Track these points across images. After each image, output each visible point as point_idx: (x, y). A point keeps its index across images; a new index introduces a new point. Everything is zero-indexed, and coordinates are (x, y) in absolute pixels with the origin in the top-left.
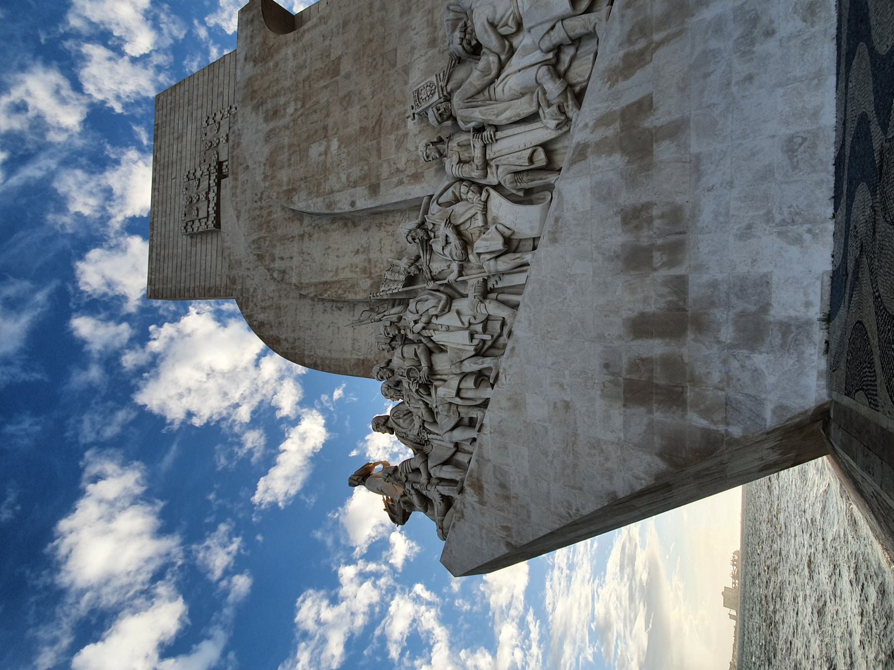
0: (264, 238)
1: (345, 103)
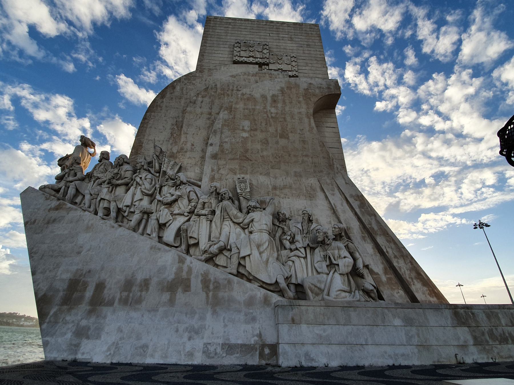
0: (216, 92)
1: (264, 141)
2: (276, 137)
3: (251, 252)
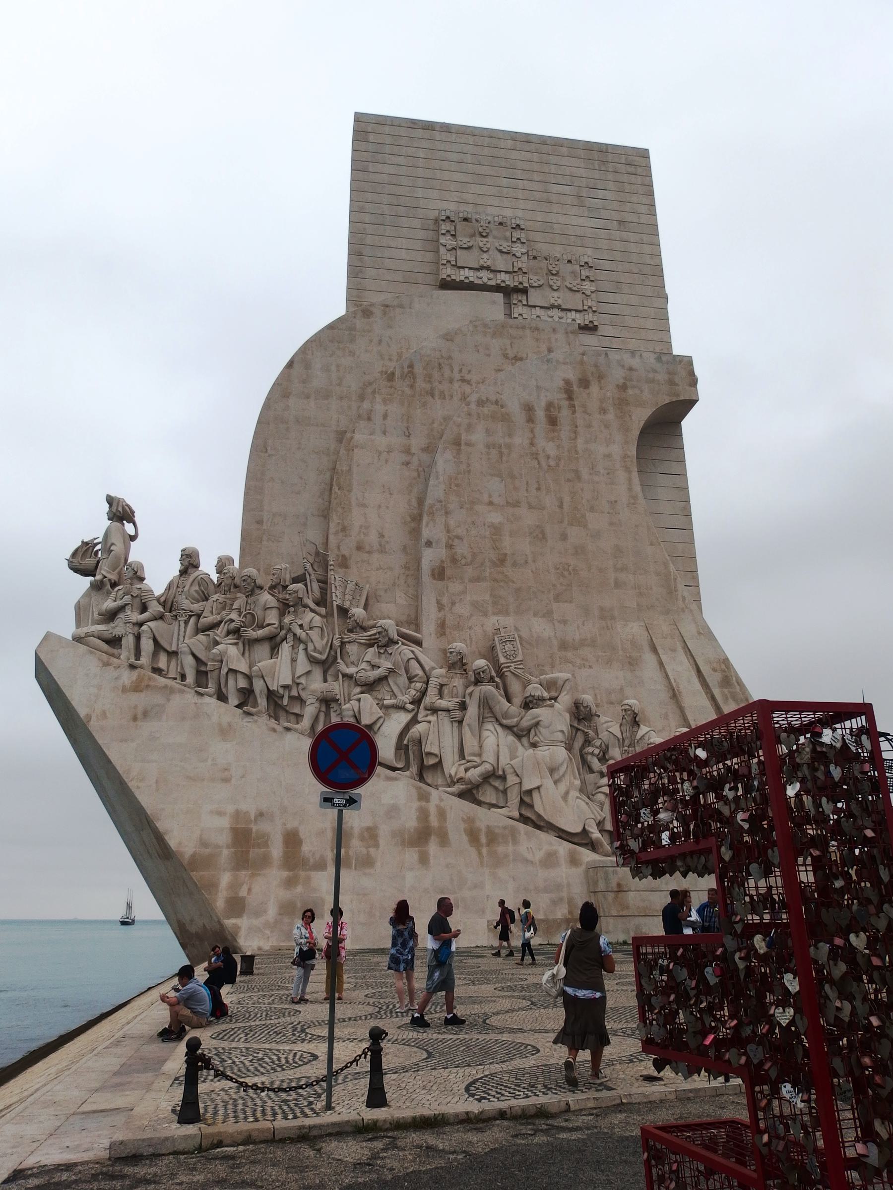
2: (562, 522)
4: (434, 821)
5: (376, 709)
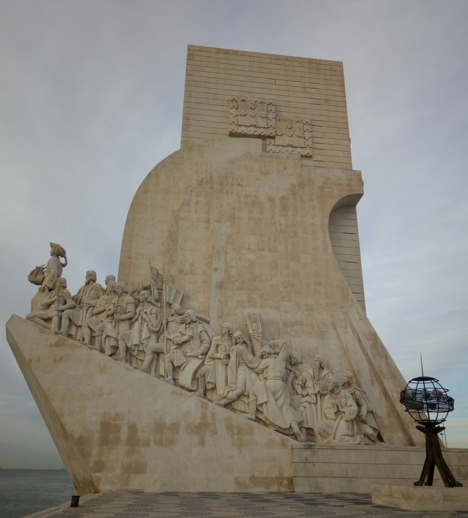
0: (212, 188)
3: (268, 399)
4: (209, 419)
5: (182, 356)
